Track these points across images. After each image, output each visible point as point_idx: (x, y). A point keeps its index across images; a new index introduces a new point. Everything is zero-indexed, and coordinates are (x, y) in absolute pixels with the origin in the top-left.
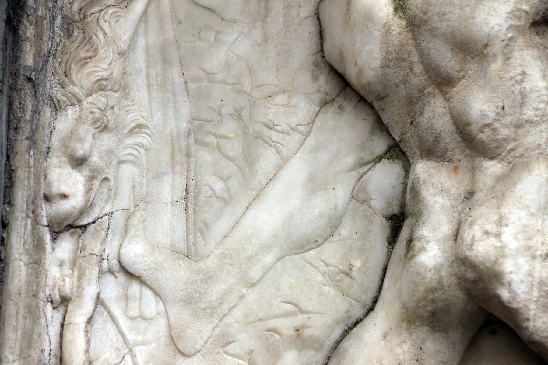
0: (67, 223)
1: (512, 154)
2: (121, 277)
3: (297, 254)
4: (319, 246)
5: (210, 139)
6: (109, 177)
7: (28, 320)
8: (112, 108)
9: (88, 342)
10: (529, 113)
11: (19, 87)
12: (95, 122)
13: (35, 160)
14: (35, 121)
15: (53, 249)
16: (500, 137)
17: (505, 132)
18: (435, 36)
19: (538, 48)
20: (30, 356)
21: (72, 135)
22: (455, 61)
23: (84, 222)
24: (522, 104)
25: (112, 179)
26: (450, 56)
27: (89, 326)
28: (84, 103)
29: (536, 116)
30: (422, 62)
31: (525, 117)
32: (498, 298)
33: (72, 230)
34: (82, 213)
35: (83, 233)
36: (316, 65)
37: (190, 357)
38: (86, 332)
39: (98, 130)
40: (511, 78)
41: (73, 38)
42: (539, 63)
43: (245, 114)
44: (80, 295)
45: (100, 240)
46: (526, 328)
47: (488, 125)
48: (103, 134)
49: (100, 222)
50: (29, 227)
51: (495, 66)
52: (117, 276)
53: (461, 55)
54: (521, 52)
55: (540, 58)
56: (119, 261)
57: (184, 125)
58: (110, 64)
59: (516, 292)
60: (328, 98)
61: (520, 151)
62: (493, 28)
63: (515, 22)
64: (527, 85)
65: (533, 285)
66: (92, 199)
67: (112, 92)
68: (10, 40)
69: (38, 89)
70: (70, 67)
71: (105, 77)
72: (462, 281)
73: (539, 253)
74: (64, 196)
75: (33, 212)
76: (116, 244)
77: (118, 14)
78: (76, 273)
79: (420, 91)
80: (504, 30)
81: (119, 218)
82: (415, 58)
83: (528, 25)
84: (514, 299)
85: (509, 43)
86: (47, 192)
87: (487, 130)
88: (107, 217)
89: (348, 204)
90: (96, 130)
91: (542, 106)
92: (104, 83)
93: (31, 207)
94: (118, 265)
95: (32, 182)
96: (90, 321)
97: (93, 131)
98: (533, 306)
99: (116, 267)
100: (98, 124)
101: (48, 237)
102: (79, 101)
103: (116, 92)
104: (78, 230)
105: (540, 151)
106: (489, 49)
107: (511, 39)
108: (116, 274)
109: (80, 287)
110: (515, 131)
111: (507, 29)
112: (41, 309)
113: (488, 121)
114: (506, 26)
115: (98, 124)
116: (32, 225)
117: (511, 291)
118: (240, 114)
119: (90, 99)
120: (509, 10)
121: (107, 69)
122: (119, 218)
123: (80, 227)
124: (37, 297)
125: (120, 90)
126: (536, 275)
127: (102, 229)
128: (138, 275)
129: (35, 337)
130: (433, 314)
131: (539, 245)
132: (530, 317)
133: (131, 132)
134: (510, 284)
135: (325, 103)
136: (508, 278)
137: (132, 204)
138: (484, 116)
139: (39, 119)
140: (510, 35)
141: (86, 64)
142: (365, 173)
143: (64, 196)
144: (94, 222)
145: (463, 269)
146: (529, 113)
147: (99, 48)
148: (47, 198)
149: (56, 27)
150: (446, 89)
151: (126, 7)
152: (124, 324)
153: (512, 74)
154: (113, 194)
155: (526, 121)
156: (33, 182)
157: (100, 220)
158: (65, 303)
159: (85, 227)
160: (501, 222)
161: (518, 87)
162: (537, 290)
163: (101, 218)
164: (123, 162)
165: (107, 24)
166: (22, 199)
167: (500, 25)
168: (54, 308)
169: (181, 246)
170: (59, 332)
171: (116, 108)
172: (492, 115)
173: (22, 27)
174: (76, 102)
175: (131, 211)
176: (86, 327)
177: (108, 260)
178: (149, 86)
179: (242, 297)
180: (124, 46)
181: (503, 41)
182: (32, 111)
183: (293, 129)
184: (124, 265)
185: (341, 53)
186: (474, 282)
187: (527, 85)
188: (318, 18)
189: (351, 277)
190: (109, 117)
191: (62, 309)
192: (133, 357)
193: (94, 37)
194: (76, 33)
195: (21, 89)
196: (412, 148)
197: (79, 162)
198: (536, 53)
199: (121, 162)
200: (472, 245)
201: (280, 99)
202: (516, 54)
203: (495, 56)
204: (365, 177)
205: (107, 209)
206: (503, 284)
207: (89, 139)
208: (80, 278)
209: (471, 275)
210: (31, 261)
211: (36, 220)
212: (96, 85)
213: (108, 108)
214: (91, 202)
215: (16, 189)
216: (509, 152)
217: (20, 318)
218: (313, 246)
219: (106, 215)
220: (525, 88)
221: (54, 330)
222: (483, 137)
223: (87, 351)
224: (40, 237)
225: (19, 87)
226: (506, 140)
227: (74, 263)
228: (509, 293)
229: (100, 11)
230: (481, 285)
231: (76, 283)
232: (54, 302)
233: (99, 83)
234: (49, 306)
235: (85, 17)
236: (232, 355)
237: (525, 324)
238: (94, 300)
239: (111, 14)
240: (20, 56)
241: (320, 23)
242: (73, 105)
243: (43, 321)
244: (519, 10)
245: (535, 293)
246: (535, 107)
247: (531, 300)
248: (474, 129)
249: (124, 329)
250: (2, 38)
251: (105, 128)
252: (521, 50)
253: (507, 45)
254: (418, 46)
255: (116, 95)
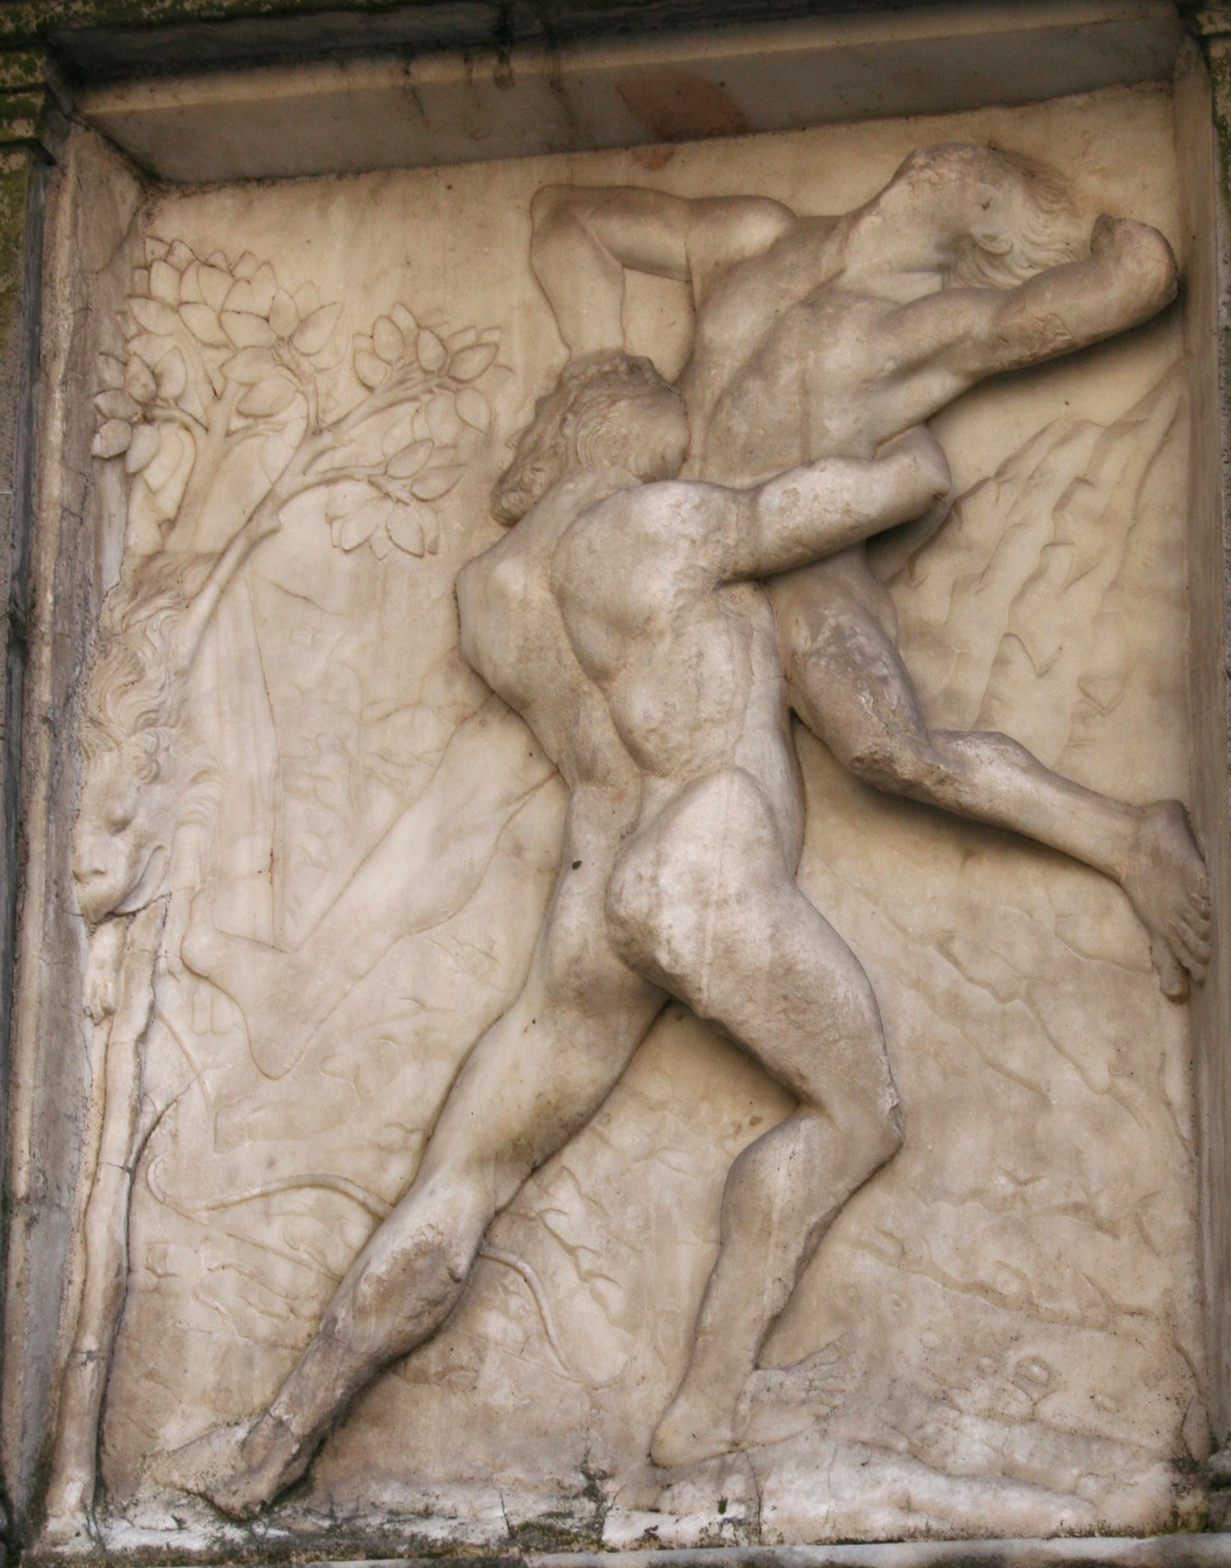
0: (105, 910)
1: (688, 767)
2: (186, 979)
3: (419, 932)
4: (450, 918)
5: (303, 783)
6: (164, 844)
7: (54, 1037)
8: (167, 749)
9: (140, 1066)
10: (708, 709)
11: (33, 731)
12: (140, 770)
13: (57, 827)
14: (57, 776)
15: (91, 946)
16: (670, 745)
17: (677, 738)
18: (585, 612)
19: (727, 617)
20: (59, 1084)
21: (110, 791)
22: (612, 645)
23: (131, 907)
24: (699, 697)
25: (169, 847)
26: (605, 638)
27: (141, 1046)
28: (124, 745)
29: (719, 712)
30: (574, 650)
31: (703, 715)
32: (654, 962)
33: (116, 920)
34: (126, 896)
35: (131, 923)
36: (451, 665)
37: (276, 1079)
38: (137, 1053)
39: (146, 781)
40: (684, 662)
41: (110, 658)
42: (724, 638)
43: (351, 745)
44: (127, 1006)
45: (154, 930)
46: (699, 1002)
47: (653, 730)
48: (152, 786)
49: (155, 907)
50: (52, 915)
51: (664, 647)
52: (180, 978)
53: (619, 636)
54: (699, 625)
55: (727, 631)
56: (181, 958)
57: (268, 765)
58: (162, 689)
59: (678, 954)
60: (468, 712)
61: (697, 762)
62: (655, 595)
63: (688, 585)
64: (706, 671)
65: (704, 942)
66: (139, 875)
67: (167, 729)
68: (17, 670)
69: (60, 732)
70: (105, 698)
71: (153, 707)
72: (614, 942)
73: (714, 898)
74: (98, 873)
75: (57, 896)
76: (177, 935)
77: (175, 618)
78: (123, 976)
79: (573, 690)
80: (670, 598)
81: (179, 899)
82: (565, 644)
83: (712, 587)
84: (676, 962)
85: (679, 614)
86: (77, 870)
87: (653, 737)
88: (164, 900)
89: (491, 858)
90: (142, 782)
91: (727, 698)
92: (153, 715)
93: (54, 889)
94: (181, 964)
95: (54, 855)
96: (143, 1038)
97: (137, 782)
98: (705, 971)
99: (178, 967)
100: (145, 773)
101: (83, 930)
102: (118, 744)
103: (172, 727)
104: (124, 919)
105: (725, 760)
106: (653, 624)
107: (681, 608)
108: (177, 976)
109: (127, 993)
110: (690, 736)
111: (676, 595)
112: (75, 1025)
113: (653, 725)
114: (672, 591)
115: (145, 773)
116: (56, 912)
117: (671, 952)
118: (344, 745)
119: (133, 739)
120: (676, 568)
121: (156, 697)
122: (179, 899)
123: (127, 915)
124: (69, 1008)
125: (179, 725)
126: (710, 928)
127: (157, 916)
128: (206, 975)
129: (67, 1060)
130: (580, 994)
131: (715, 888)
132: (702, 986)
133: (195, 781)
134: (669, 942)
135: (463, 720)
136: (665, 934)
137: (198, 880)
138: (648, 718)
139: (62, 772)
140: (680, 603)
141: (125, 692)
142: (517, 812)
143: (98, 873)
144: (145, 908)
145: (612, 927)
146: (708, 709)
147: (146, 668)
148: (77, 877)
149: (88, 646)
150: (606, 685)
151: (187, 607)
152: (188, 1041)
153: (685, 656)
154: (170, 868)
155: (705, 720)
156: (57, 855)
157: (153, 904)
158: (110, 1017)
159: (134, 914)
160: (659, 862)
161: (692, 674)
162: (711, 949)
163: (155, 901)
164: (184, 823)
165: (157, 634)
166: (39, 878)
167: (665, 591)
168: (96, 1025)
169: (265, 935)
170: (103, 1056)
171: (171, 749)
172: (658, 715)
173: (35, 650)
174: (113, 745)
175: (197, 889)
176: (137, 1047)
177: (166, 958)
178: (220, 714)
179: (345, 995)
180: (184, 662)
181: (670, 612)
182: (50, 762)
183: (418, 759)
184: (187, 962)
185: (475, 647)
186: (627, 944)
187: (706, 671)
188: (456, 599)
189: (492, 958)
190: (161, 762)
191: (106, 1025)
192: (202, 1084)
193: (139, 654)
194: (115, 651)
195: (36, 734)
196: (569, 772)
197: (120, 826)
198: (722, 624)
199: (180, 824)
200: (620, 894)
201: (401, 719)
202: (691, 629)
203: (661, 634)
204: (519, 818)
205: (163, 889)
206: (660, 943)
207: (133, 793)
208: (127, 982)
209: (620, 935)
210: (56, 960)
211: (62, 907)
212: (141, 721)
213: (161, 750)
214: (138, 880)
215: (30, 864)
216: (682, 766)
217: (42, 1032)
218: (442, 919)
219: (163, 896)
220: (702, 675)
221: (96, 1052)
222: (650, 747)
223: (139, 1077)
224: (69, 929)
225: (33, 731)
226: (679, 748)
227: (119, 963)
228: (669, 954)
229: (149, 617)
230: (636, 948)
231: (123, 989)
232: (95, 1016)
233: (145, 717)
234: (88, 1023)
235: (128, 627)
236: (333, 1074)
237: (696, 996)
238: (146, 1011)
239: (164, 620)
240: (33, 690)
241: (457, 607)
242: (110, 750)
243: (79, 1041)
244: (693, 567)
245: (709, 954)
246: (717, 700)
247: (701, 963)
248: (638, 737)
249: (189, 1048)
250: (4, 669)
251: (155, 778)
252: (699, 622)
253: (678, 617)
254: (567, 626)
255: (173, 731)
